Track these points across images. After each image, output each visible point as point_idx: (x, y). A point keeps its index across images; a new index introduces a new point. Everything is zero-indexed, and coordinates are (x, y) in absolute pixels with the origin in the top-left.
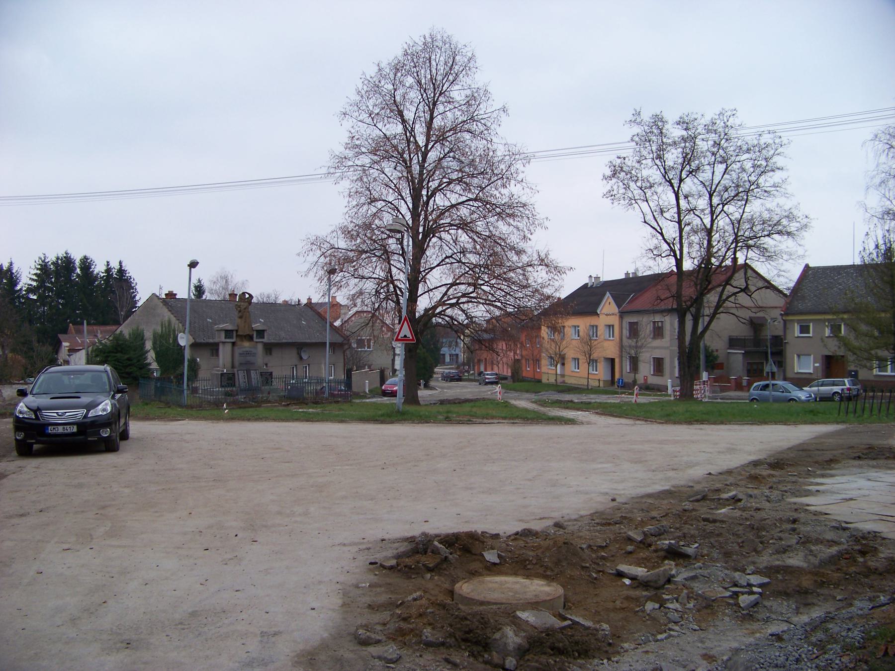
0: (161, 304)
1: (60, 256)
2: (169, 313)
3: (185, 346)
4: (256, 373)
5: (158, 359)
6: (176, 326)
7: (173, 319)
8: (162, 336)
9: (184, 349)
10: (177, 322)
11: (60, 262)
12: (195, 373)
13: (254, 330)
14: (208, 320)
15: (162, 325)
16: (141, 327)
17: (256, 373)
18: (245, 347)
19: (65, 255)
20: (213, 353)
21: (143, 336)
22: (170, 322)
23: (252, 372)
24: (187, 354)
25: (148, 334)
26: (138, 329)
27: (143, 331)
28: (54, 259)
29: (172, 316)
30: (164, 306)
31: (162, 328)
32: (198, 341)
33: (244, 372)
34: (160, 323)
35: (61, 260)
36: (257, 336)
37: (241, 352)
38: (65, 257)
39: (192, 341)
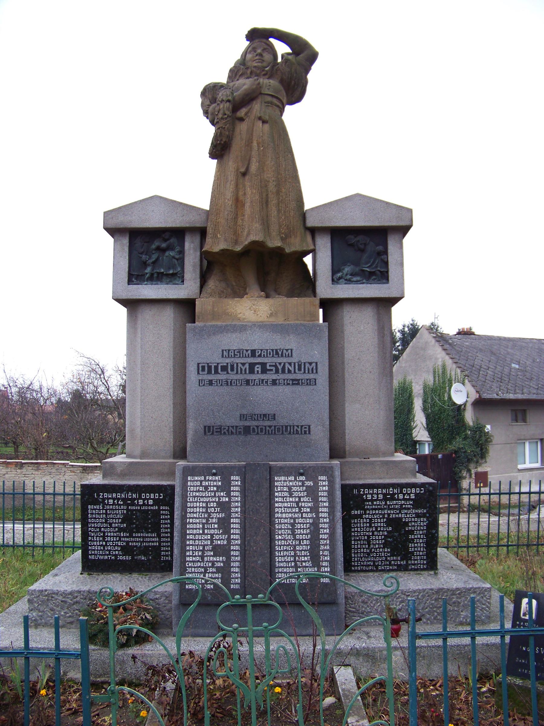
0: (433, 341)
1: (407, 323)
2: (443, 353)
3: (465, 404)
4: (313, 492)
5: (430, 429)
6: (453, 373)
7: (449, 362)
8: (434, 390)
9: (464, 410)
10: (454, 366)
11: (406, 329)
12: (482, 449)
13: (314, 231)
14: (513, 365)
15: (434, 372)
16: (409, 378)
17: (313, 492)
18: (242, 328)
19: (411, 322)
20: (516, 416)
21: (411, 392)
22: (444, 367)
23: (280, 481)
24: (469, 417)
25: (417, 389)
26: (405, 380)
27: (411, 382)
28: (401, 328)
29: (447, 358)
30: (437, 344)
31: (434, 377)
32: (485, 396)
33: (226, 487)
34: (432, 370)
35: (408, 327)
36: (334, 271)
37: (216, 359)
38: (411, 325)
39: (474, 396)
